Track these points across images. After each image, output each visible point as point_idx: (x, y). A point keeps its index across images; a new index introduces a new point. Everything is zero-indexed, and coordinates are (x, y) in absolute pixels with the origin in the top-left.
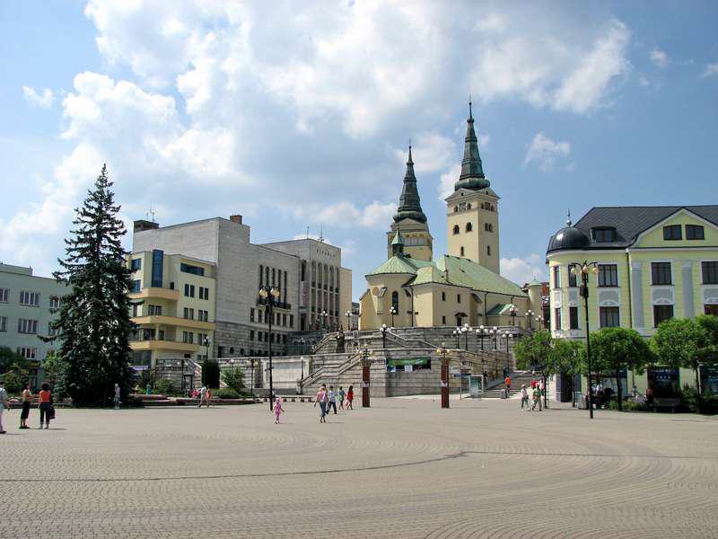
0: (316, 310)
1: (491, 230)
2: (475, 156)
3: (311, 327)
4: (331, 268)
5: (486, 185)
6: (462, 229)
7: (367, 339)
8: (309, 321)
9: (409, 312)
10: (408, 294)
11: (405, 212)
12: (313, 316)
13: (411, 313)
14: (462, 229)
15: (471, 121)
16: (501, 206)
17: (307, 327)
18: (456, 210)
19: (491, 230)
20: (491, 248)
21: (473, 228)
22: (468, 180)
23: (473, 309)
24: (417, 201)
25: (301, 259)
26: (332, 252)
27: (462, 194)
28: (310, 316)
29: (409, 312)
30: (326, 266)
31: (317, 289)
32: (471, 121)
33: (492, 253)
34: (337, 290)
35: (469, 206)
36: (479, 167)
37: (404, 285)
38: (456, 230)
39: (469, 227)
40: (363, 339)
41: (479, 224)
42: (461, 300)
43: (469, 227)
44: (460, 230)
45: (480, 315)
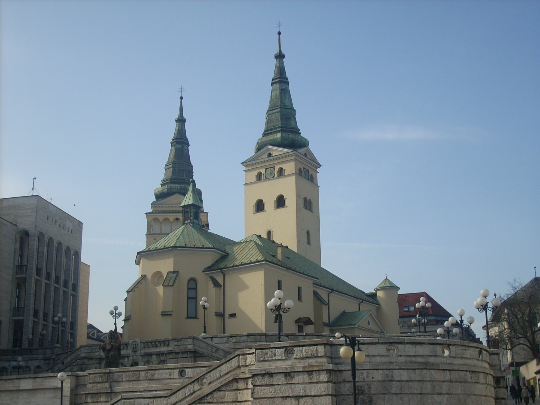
0: (41, 315)
1: (310, 209)
2: (287, 103)
3: (31, 342)
4: (68, 249)
5: (304, 144)
6: (270, 204)
7: (158, 354)
8: (28, 334)
9: (218, 314)
10: (216, 284)
11: (174, 186)
12: (35, 323)
13: (220, 315)
14: (270, 204)
15: (280, 56)
16: (322, 176)
17: (25, 345)
18: (259, 177)
19: (310, 209)
20: (311, 233)
21: (287, 202)
22: (279, 135)
23: (318, 312)
24: (190, 171)
25: (21, 227)
26: (69, 225)
27: (270, 155)
28: (31, 325)
29: (218, 314)
30: (60, 244)
31: (44, 281)
32: (280, 56)
33: (311, 243)
34: (75, 287)
35: (281, 171)
36: (292, 119)
37: (209, 269)
38: (260, 206)
39: (280, 202)
40: (151, 355)
41: (298, 196)
42: (303, 298)
43: (280, 202)
44: (266, 207)
45: (325, 324)
